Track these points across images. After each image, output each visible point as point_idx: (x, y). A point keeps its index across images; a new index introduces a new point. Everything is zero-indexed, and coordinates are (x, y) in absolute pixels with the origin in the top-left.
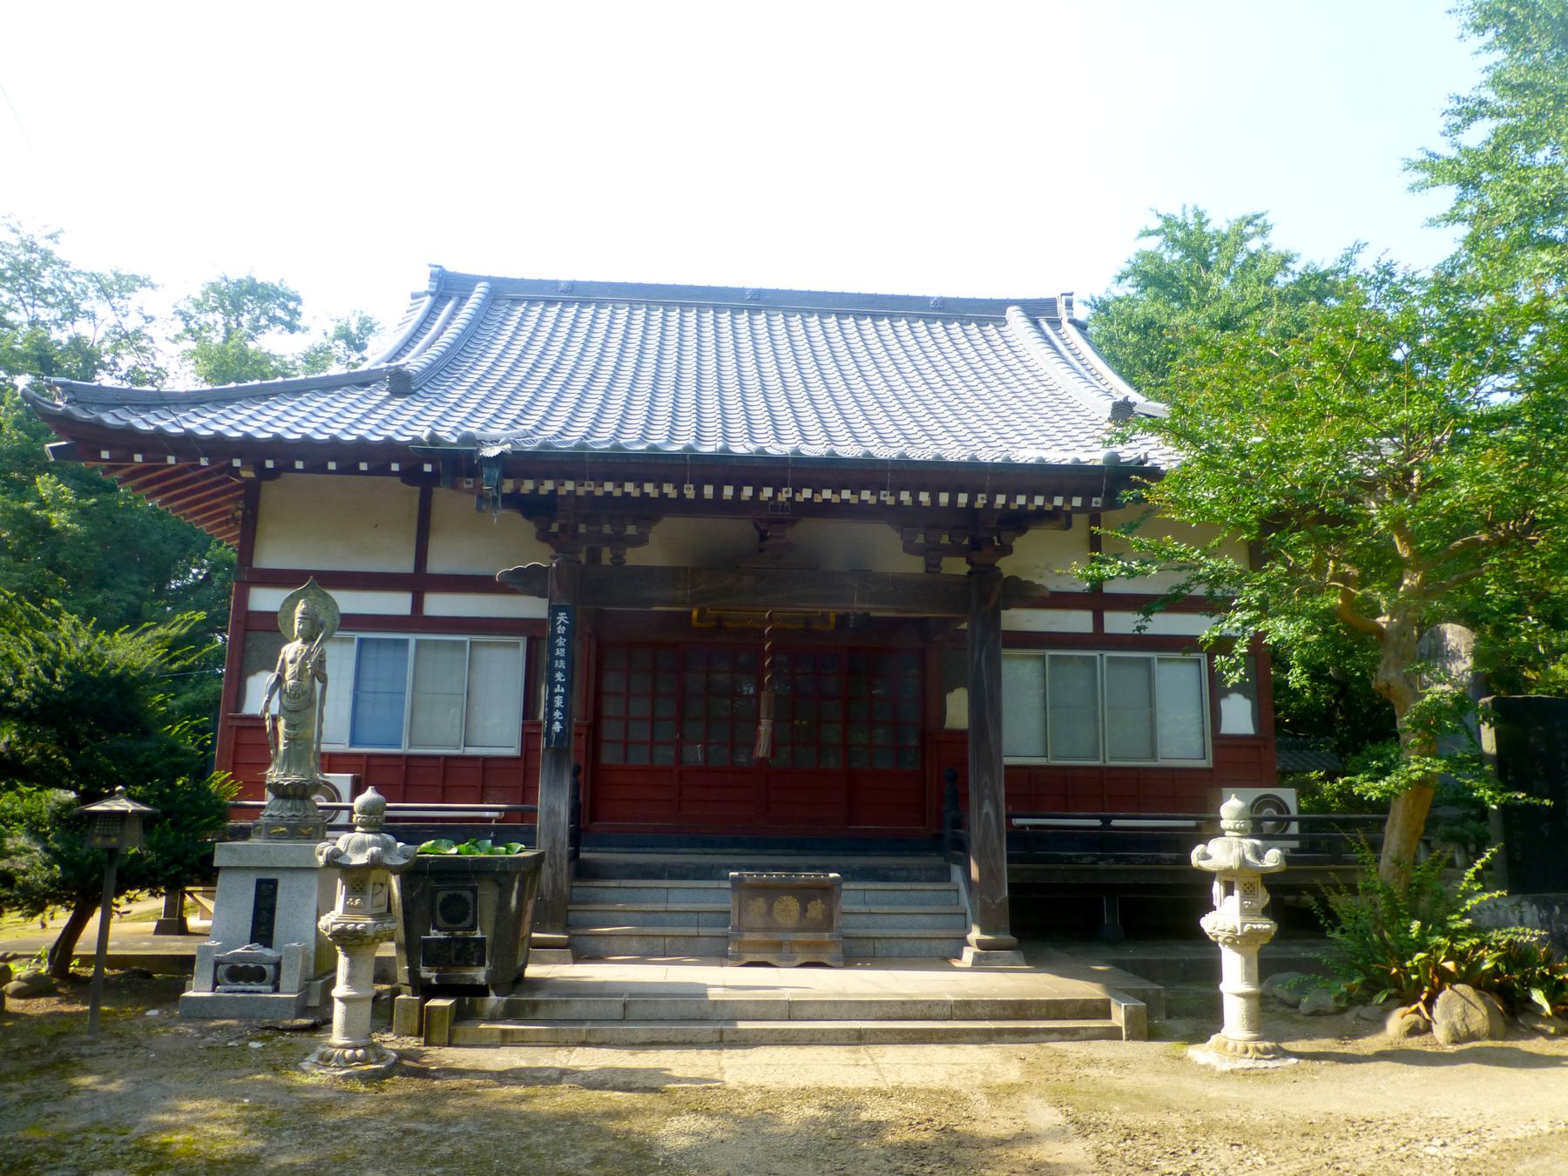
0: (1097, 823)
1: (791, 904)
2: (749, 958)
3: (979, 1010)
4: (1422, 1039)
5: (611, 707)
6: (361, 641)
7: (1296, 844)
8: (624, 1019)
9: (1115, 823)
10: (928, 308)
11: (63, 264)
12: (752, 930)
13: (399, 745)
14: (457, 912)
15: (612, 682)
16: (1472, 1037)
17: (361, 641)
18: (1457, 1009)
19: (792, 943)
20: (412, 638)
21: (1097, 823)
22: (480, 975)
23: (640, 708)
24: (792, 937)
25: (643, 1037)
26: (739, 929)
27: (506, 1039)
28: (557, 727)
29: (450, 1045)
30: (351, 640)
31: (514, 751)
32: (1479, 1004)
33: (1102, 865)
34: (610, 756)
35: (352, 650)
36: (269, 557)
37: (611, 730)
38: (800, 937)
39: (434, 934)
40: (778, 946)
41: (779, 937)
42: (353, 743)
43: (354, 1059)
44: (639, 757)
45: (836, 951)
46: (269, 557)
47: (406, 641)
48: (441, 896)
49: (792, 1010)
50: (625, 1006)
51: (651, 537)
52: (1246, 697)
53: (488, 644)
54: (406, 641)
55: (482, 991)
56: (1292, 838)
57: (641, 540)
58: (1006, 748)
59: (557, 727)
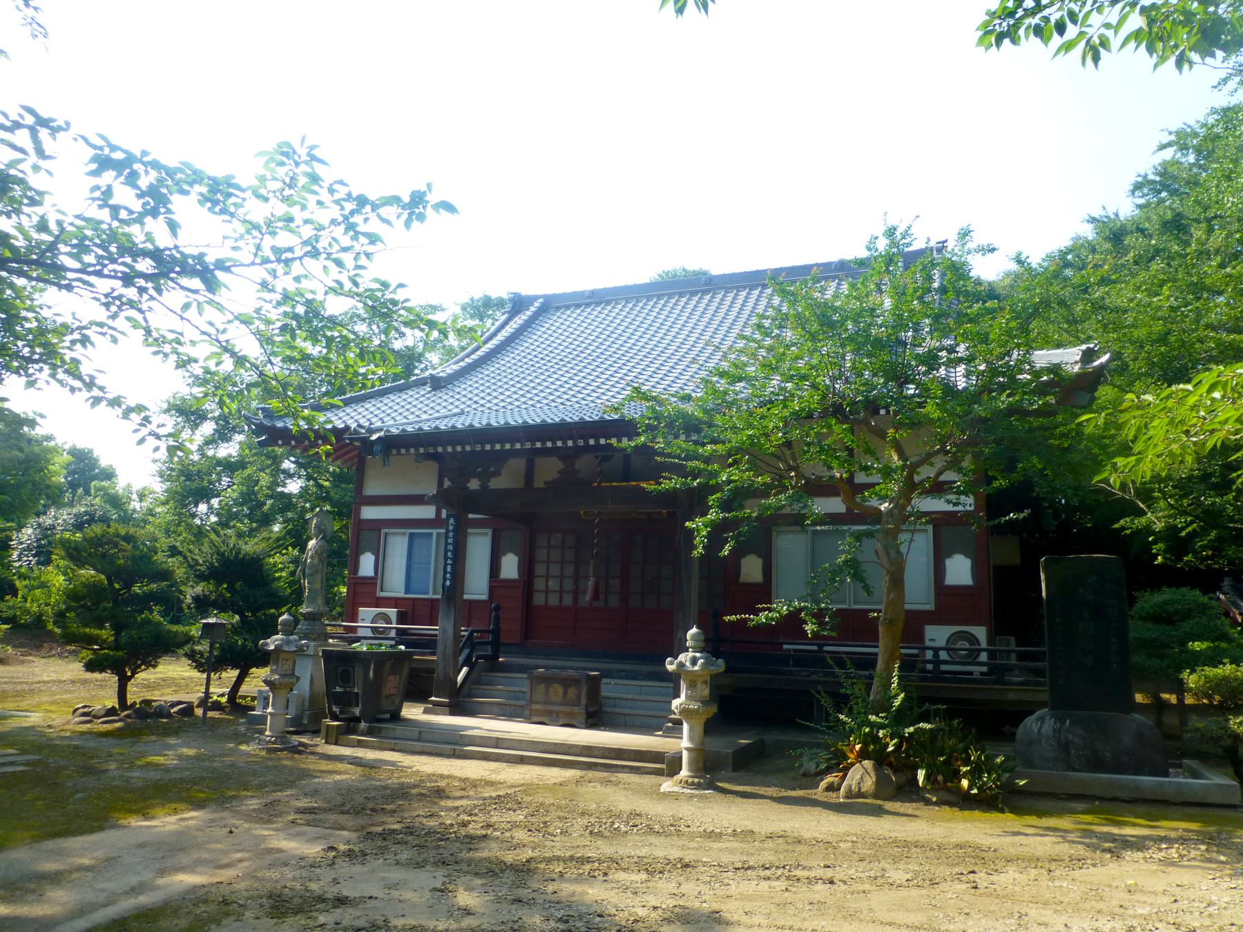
0: (815, 648)
1: (559, 689)
2: (539, 719)
3: (596, 752)
4: (834, 795)
5: (540, 569)
6: (411, 535)
7: (985, 669)
8: (419, 740)
9: (826, 648)
10: (831, 271)
11: (102, 389)
12: (537, 703)
13: (427, 593)
14: (346, 679)
15: (541, 554)
16: (860, 794)
17: (411, 535)
18: (861, 775)
19: (558, 713)
20: (434, 531)
21: (815, 648)
22: (357, 711)
23: (555, 570)
24: (557, 708)
25: (419, 749)
26: (531, 702)
27: (360, 744)
28: (448, 583)
29: (336, 744)
30: (404, 534)
31: (484, 597)
32: (873, 774)
33: (814, 677)
34: (539, 599)
35: (406, 539)
36: (371, 489)
37: (539, 584)
38: (562, 708)
39: (338, 689)
40: (550, 713)
41: (552, 708)
42: (407, 591)
43: (270, 742)
44: (553, 600)
45: (582, 718)
46: (371, 489)
47: (431, 534)
48: (340, 669)
49: (498, 742)
50: (420, 733)
51: (503, 471)
52: (966, 556)
53: (395, 534)
54: (431, 534)
55: (358, 720)
56: (982, 664)
57: (497, 473)
58: (466, 590)
59: (448, 583)
